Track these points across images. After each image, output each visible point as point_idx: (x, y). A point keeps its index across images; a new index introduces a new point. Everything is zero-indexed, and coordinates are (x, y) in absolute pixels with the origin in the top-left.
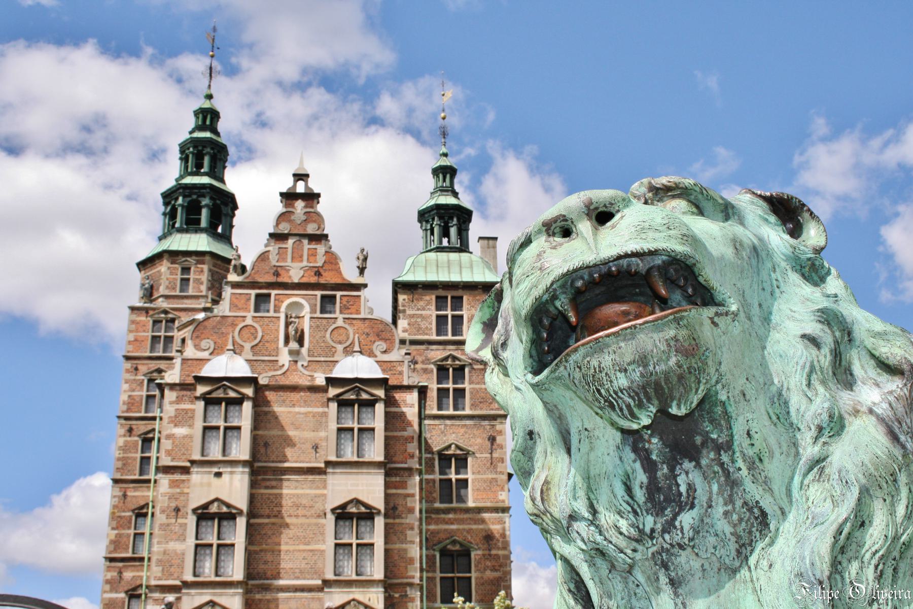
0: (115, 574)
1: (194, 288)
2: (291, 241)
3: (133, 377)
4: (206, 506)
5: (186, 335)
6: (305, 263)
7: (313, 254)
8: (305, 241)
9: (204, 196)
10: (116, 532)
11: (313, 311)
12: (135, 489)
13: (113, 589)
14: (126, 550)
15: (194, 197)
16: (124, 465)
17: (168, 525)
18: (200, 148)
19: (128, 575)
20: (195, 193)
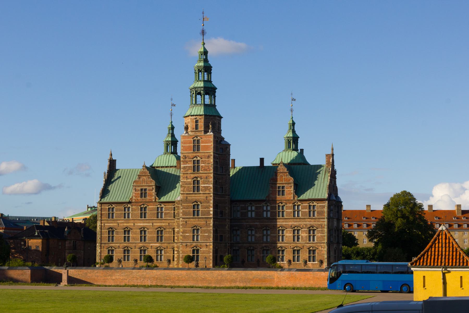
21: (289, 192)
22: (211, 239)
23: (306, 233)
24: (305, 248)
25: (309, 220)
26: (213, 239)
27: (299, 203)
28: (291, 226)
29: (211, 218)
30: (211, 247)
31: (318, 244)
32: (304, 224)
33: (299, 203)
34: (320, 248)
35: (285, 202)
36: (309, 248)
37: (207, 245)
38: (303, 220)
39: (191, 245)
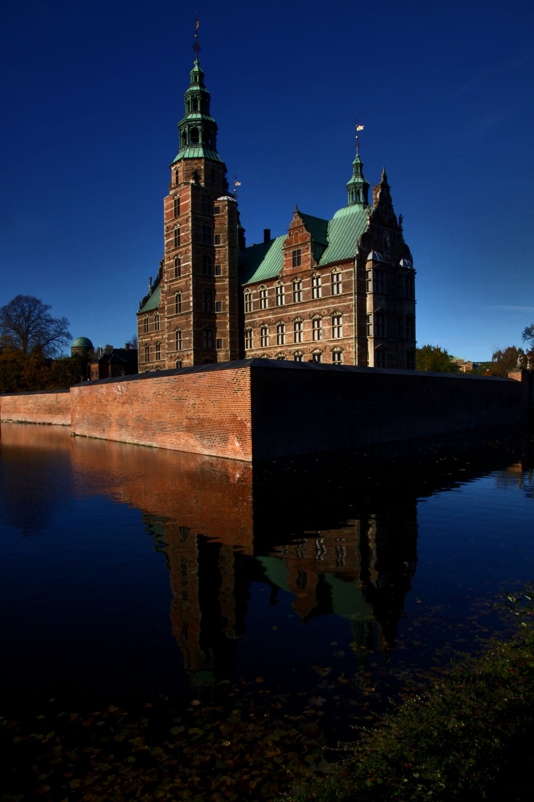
5: (221, 206)
21: (306, 257)
22: (192, 345)
23: (329, 324)
24: (328, 350)
25: (332, 300)
26: (194, 346)
27: (318, 274)
28: (310, 315)
29: (190, 313)
30: (192, 357)
31: (345, 342)
32: (326, 309)
33: (318, 274)
35: (301, 275)
37: (188, 355)
38: (324, 302)
39: (175, 356)
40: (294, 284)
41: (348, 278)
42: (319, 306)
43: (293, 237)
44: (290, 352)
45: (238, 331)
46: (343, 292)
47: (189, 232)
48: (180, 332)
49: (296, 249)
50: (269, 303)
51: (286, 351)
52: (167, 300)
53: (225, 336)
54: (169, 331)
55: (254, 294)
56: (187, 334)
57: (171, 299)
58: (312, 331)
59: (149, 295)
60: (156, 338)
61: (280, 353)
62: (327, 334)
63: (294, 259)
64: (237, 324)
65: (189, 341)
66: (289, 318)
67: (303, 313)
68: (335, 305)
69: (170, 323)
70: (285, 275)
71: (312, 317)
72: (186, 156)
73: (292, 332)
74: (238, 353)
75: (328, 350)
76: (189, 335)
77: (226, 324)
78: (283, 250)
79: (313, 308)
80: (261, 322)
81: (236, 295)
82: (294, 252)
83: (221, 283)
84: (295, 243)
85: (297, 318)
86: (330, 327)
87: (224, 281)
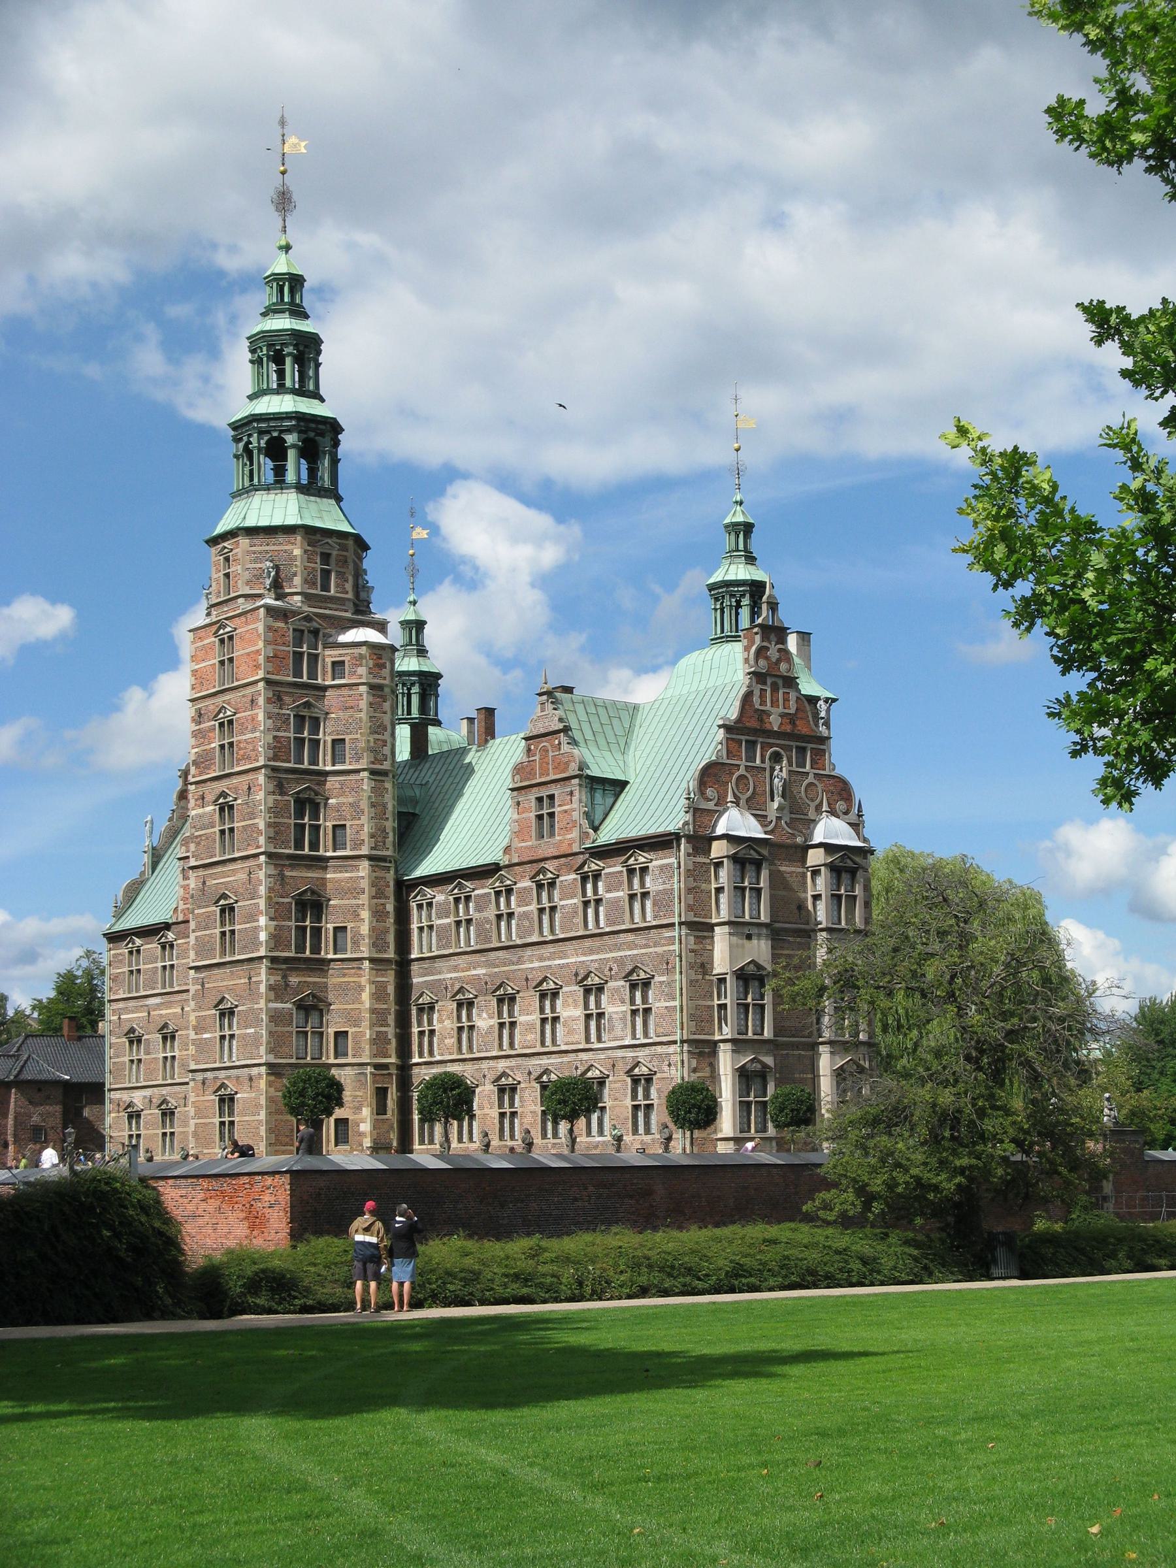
0: (279, 978)
1: (337, 586)
2: (769, 681)
3: (277, 711)
4: (742, 969)
5: (346, 659)
6: (781, 709)
7: (786, 700)
8: (780, 682)
9: (322, 435)
10: (275, 923)
11: (790, 764)
12: (292, 867)
13: (278, 998)
14: (288, 948)
15: (312, 434)
16: (276, 833)
17: (697, 981)
18: (301, 348)
19: (294, 980)
20: (313, 430)
22: (263, 1049)
23: (623, 1002)
25: (630, 937)
28: (576, 975)
29: (261, 958)
30: (263, 1084)
32: (615, 959)
34: (666, 1068)
35: (556, 862)
36: (629, 1072)
37: (251, 1079)
40: (540, 886)
41: (664, 883)
42: (599, 950)
43: (537, 758)
44: (530, 1073)
45: (393, 1008)
46: (655, 917)
47: (258, 734)
48: (232, 1013)
49: (544, 792)
50: (478, 936)
51: (518, 1067)
52: (196, 917)
53: (357, 1023)
54: (200, 1008)
55: (439, 904)
56: (251, 1019)
57: (209, 916)
58: (583, 1018)
59: (143, 873)
60: (163, 1012)
61: (504, 1074)
62: (618, 1025)
63: (540, 817)
64: (391, 989)
65: (256, 1038)
66: (527, 979)
67: (561, 967)
68: (635, 952)
69: (203, 985)
70: (516, 860)
71: (582, 981)
72: (251, 522)
73: (534, 1017)
74: (394, 1071)
75: (622, 1068)
76: (257, 1022)
77: (361, 988)
78: (512, 790)
79: (584, 954)
80: (457, 987)
81: (390, 907)
82: (540, 800)
83: (347, 875)
84: (541, 775)
85: (545, 979)
86: (624, 1009)
87: (356, 868)
